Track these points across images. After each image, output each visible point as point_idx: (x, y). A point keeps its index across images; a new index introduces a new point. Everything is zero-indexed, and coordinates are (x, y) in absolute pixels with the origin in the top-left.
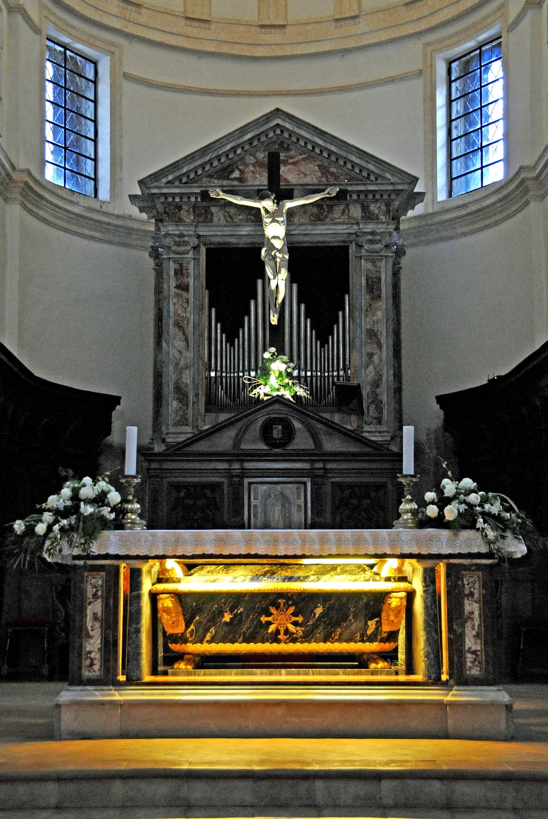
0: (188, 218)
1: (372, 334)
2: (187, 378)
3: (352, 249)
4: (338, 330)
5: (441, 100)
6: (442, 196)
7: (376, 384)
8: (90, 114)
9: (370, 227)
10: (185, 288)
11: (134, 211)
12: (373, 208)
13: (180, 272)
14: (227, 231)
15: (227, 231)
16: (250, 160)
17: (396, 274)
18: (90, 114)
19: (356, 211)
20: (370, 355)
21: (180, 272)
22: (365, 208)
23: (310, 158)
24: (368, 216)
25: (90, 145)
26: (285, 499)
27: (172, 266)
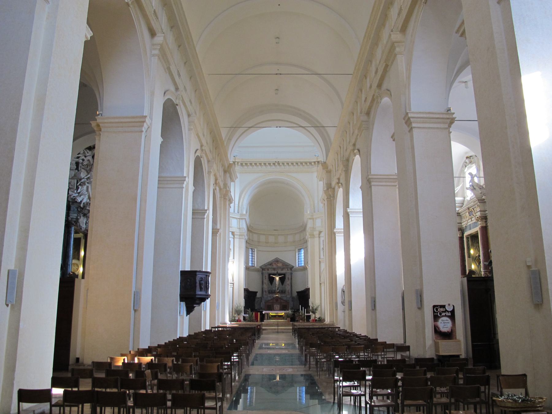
0: (266, 270)
1: (288, 284)
2: (266, 290)
3: (286, 274)
4: (284, 284)
5: (297, 254)
6: (297, 266)
7: (289, 290)
8: (254, 256)
9: (288, 271)
10: (266, 279)
11: (259, 268)
12: (289, 269)
13: (265, 277)
14: (271, 272)
15: (271, 272)
16: (274, 263)
17: (291, 276)
18: (254, 256)
19: (286, 269)
20: (288, 287)
21: (265, 277)
22: (287, 269)
23: (281, 263)
24: (288, 270)
25: (254, 260)
26: (278, 306)
27: (264, 276)
